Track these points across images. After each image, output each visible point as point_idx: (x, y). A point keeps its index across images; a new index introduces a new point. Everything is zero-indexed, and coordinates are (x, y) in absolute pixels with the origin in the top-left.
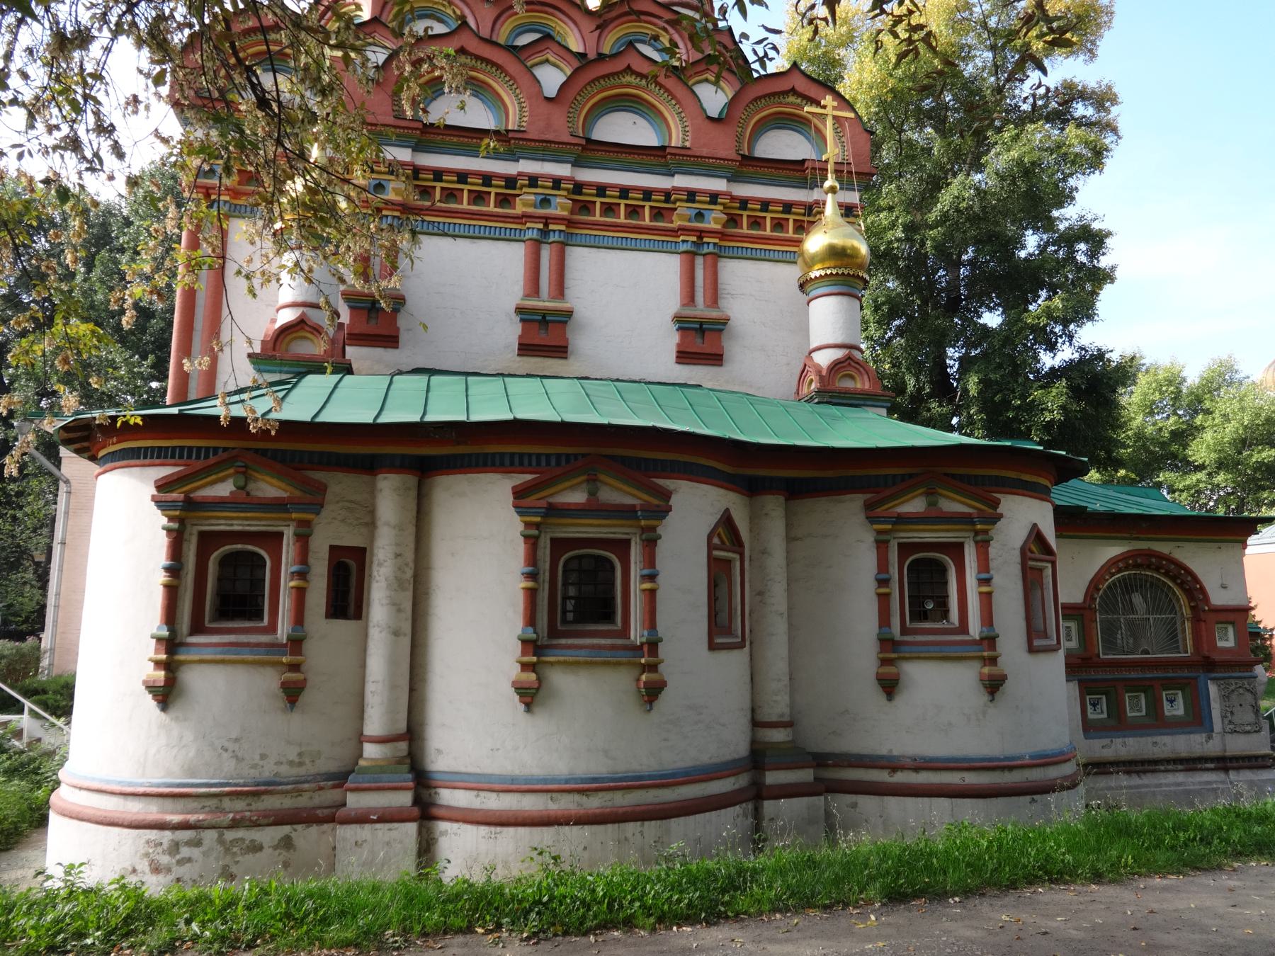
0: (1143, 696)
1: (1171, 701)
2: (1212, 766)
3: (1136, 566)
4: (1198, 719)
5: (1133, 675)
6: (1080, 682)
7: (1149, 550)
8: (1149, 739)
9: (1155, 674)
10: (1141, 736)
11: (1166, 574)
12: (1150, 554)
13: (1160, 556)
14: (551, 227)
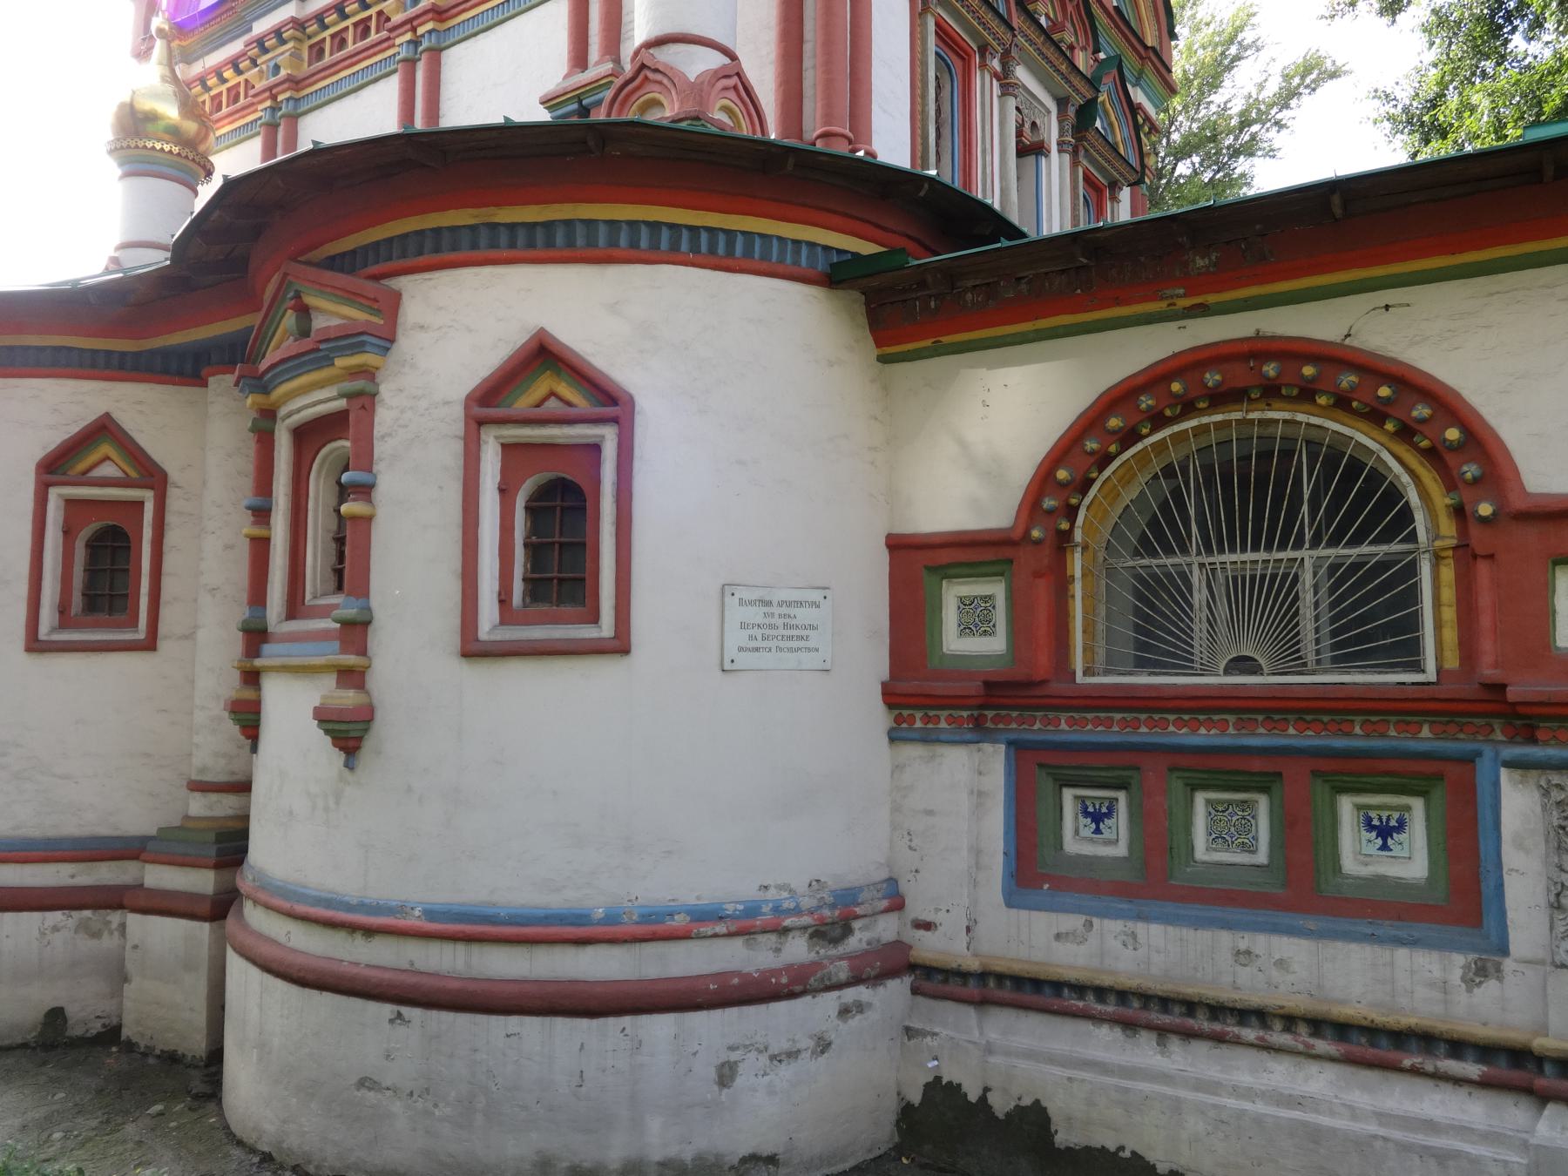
0: (1263, 803)
1: (1385, 832)
2: (1472, 1069)
3: (1220, 398)
4: (1461, 903)
5: (1205, 736)
6: (1019, 751)
7: (1258, 337)
8: (1225, 939)
9: (1292, 736)
10: (1198, 924)
11: (1342, 403)
12: (1259, 350)
13: (1293, 352)
14: (421, 30)
